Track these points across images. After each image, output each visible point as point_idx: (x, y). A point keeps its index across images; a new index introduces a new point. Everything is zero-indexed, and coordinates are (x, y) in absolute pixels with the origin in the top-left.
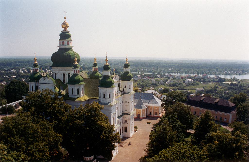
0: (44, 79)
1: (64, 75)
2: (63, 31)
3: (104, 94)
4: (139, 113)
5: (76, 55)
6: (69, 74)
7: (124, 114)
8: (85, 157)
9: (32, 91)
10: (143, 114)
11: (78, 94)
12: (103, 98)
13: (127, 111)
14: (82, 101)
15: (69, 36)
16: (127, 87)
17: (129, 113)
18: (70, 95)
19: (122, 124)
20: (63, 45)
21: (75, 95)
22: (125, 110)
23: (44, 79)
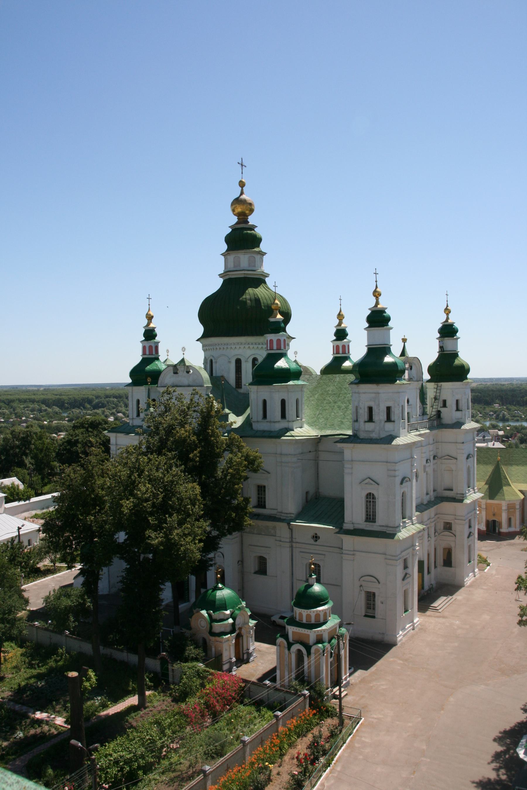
1: (238, 362)
2: (237, 224)
3: (370, 409)
4: (494, 515)
6: (255, 360)
7: (440, 499)
8: (300, 610)
9: (138, 415)
10: (510, 520)
12: (365, 422)
13: (452, 490)
14: (297, 438)
15: (256, 241)
16: (451, 404)
17: (458, 497)
19: (435, 536)
20: (235, 269)
21: (274, 422)
22: (443, 489)
23: (176, 371)
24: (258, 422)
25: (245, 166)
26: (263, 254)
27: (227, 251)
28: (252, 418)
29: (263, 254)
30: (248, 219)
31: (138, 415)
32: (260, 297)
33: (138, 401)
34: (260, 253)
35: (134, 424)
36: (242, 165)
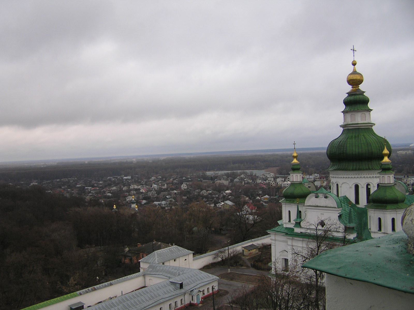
0: (315, 197)
1: (357, 187)
5: (383, 142)
6: (368, 185)
9: (290, 221)
11: (393, 229)
15: (365, 102)
18: (375, 232)
24: (375, 232)
25: (356, 51)
26: (370, 110)
27: (345, 109)
28: (370, 229)
29: (370, 110)
30: (359, 87)
31: (290, 221)
32: (371, 143)
33: (289, 212)
34: (369, 110)
35: (287, 227)
36: (354, 50)
